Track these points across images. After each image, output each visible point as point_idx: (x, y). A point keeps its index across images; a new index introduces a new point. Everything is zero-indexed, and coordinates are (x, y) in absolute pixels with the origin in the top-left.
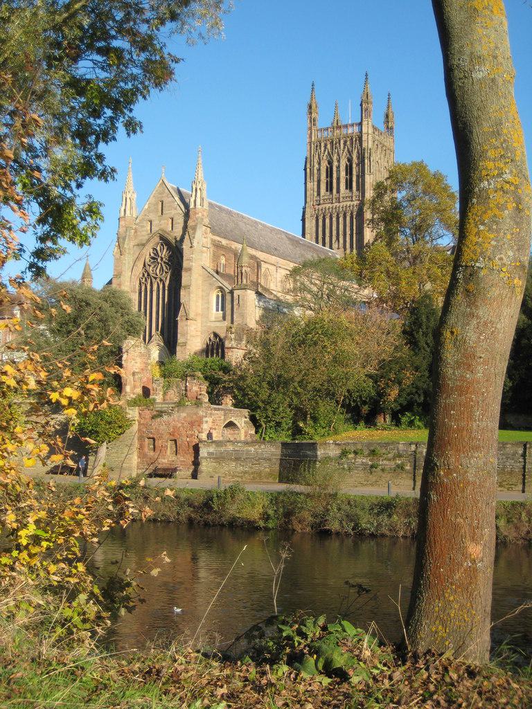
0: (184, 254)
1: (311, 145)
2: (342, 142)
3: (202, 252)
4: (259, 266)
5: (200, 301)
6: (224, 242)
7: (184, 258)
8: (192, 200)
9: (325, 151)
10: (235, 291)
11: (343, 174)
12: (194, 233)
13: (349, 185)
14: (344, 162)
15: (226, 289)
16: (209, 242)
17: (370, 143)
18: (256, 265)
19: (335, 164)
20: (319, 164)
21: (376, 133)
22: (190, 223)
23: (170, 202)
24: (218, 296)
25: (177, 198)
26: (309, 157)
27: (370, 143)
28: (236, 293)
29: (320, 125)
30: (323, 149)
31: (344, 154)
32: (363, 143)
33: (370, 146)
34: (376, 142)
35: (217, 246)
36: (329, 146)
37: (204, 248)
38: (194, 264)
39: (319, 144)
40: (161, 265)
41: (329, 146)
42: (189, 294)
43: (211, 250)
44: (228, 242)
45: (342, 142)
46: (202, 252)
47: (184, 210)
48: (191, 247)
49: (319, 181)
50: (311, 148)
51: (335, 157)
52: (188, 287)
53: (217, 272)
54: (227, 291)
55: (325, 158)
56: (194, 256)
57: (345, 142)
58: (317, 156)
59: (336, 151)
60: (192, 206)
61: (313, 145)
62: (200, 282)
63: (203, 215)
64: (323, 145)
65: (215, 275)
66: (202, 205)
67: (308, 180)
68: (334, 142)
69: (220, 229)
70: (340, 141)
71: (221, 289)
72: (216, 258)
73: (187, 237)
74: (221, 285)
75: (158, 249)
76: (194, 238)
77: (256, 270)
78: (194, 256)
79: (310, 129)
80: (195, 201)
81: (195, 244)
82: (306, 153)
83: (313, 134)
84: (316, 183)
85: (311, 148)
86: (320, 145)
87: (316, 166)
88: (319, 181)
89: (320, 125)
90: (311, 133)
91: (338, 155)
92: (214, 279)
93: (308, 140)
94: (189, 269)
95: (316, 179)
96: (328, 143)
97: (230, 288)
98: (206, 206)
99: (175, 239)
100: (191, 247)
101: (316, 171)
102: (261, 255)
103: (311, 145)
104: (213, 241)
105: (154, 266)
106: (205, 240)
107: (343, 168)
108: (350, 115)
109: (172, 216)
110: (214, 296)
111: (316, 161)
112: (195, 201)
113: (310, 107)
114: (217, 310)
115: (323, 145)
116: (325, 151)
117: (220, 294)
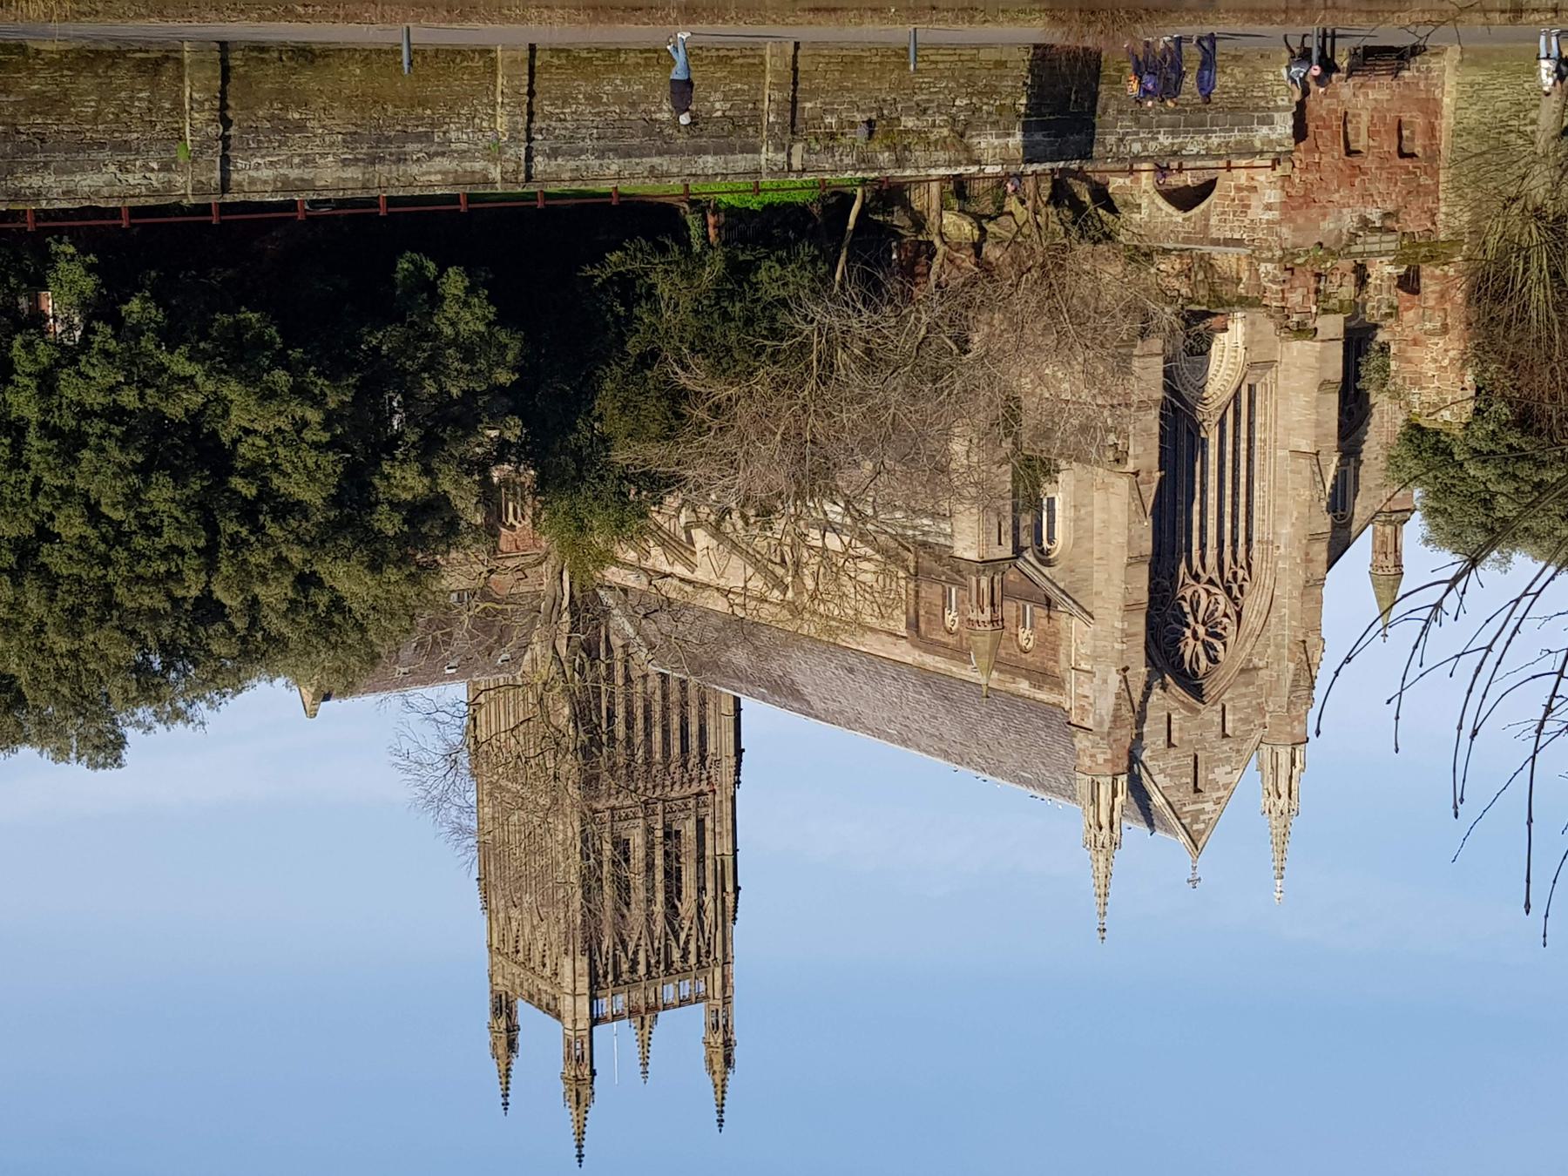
0: (1142, 655)
1: (725, 955)
2: (642, 969)
3: (1095, 658)
4: (914, 625)
5: (1097, 525)
6: (1023, 686)
7: (1142, 640)
8: (1120, 798)
9: (687, 942)
10: (1009, 554)
11: (638, 881)
12: (1118, 708)
13: (622, 846)
14: (636, 914)
15: (1032, 559)
16: (1072, 685)
17: (567, 971)
18: (923, 626)
19: (659, 908)
20: (700, 907)
21: (545, 999)
22: (1126, 735)
23: (1178, 787)
24: (1050, 541)
25: (1157, 800)
26: (729, 924)
27: (567, 971)
28: (1007, 551)
29: (697, 1015)
30: (692, 947)
31: (635, 937)
32: (586, 967)
33: (567, 962)
34: (548, 972)
35: (1045, 677)
36: (676, 955)
37: (1088, 667)
38: (1118, 625)
39: (703, 959)
40: (1197, 622)
41: (676, 955)
42: (1129, 543)
43: (1064, 664)
44: (1012, 687)
45: (642, 969)
46: (1095, 658)
47: (1144, 774)
48: (1125, 669)
49: (701, 859)
50: (724, 950)
51: (659, 927)
52: (1133, 561)
53: (1049, 603)
54: (1028, 555)
55: (686, 924)
56: (1118, 646)
57: (633, 969)
58: (707, 929)
59: (656, 945)
60: (1123, 779)
61: (719, 955)
62: (1099, 576)
63: (1092, 756)
64: (692, 959)
65: (1055, 594)
66: (1095, 786)
67: (729, 861)
68: (662, 967)
69: (1028, 721)
70: (649, 972)
71: (1044, 558)
72: (1050, 643)
73: (1137, 697)
74: (1046, 570)
75: (1203, 662)
76: (1118, 696)
77: (922, 612)
78: (1118, 646)
79: (726, 1001)
80: (1115, 794)
81: (1115, 679)
82: (738, 931)
83: (718, 983)
84: (709, 852)
85: (724, 950)
86: (699, 955)
87: (708, 899)
88: (701, 859)
89: (697, 1015)
90: (724, 987)
91: (651, 933)
92: (1061, 585)
93: (735, 969)
94: (1129, 608)
95: (709, 862)
96: (678, 965)
97: (1020, 563)
98: (1083, 782)
99: (1164, 687)
100: (1125, 669)
101: (710, 886)
102: (906, 653)
103: (725, 955)
104: (1058, 684)
105: (1212, 614)
106: (1086, 690)
107: (639, 894)
108: (613, 1041)
109: (1172, 751)
110: (1061, 540)
111: (710, 914)
112: (1115, 794)
113: (728, 1061)
114: (1051, 501)
115: (692, 959)
116: (687, 942)
117: (1045, 545)
